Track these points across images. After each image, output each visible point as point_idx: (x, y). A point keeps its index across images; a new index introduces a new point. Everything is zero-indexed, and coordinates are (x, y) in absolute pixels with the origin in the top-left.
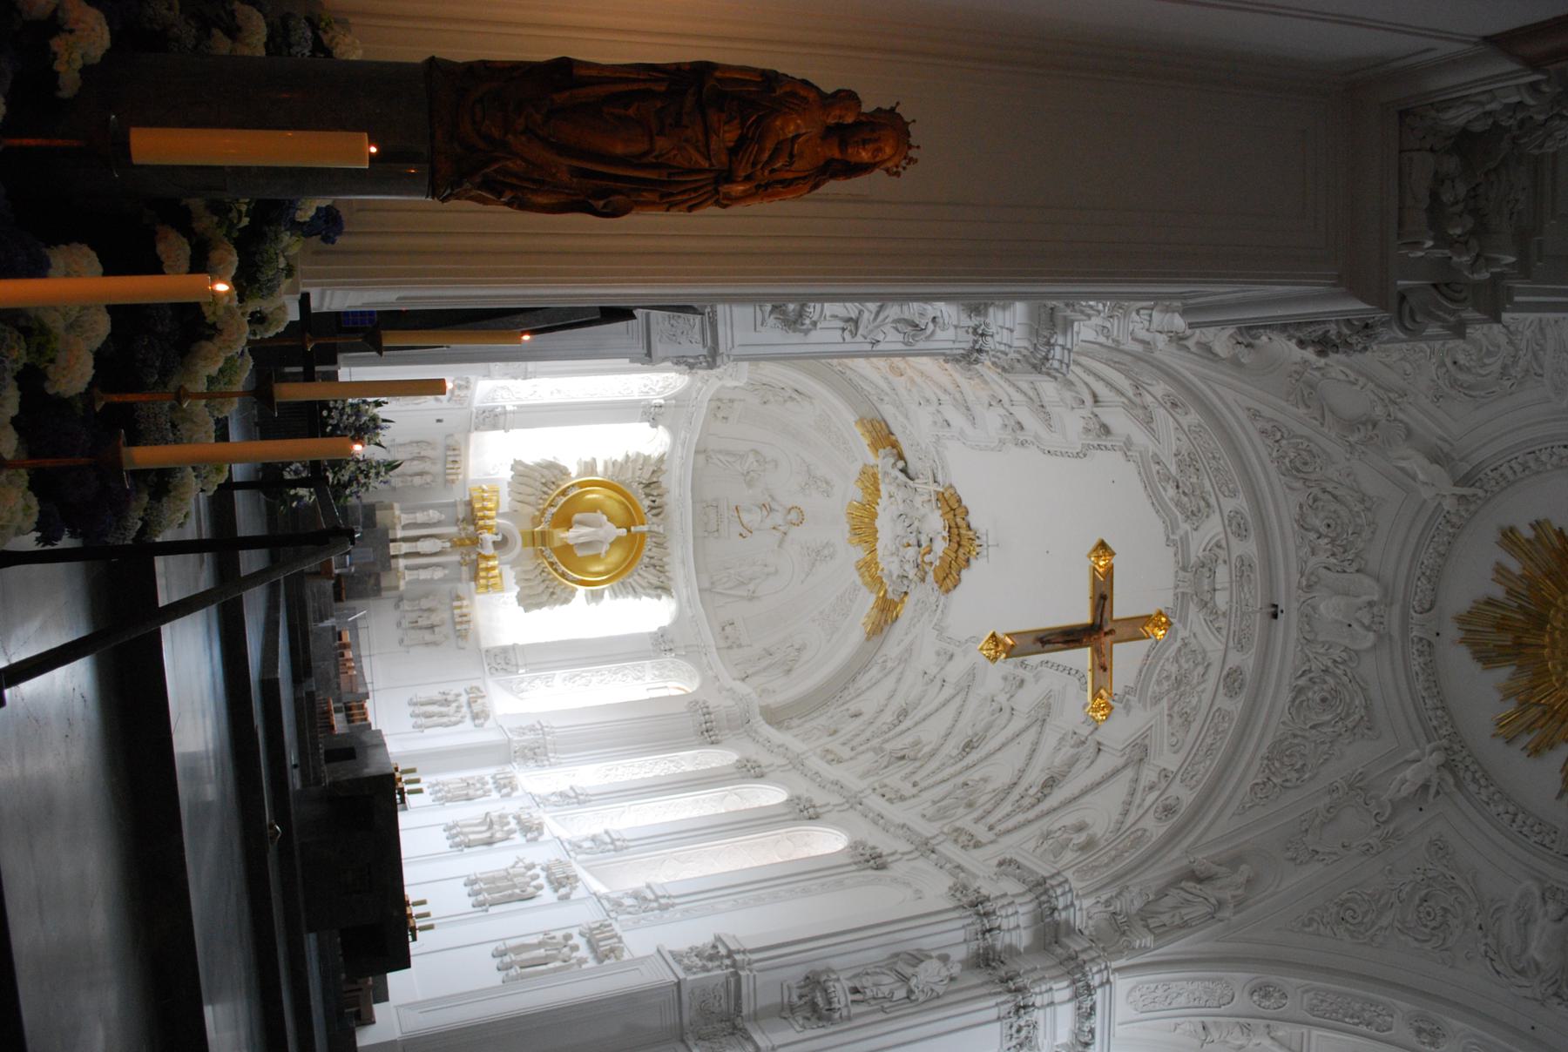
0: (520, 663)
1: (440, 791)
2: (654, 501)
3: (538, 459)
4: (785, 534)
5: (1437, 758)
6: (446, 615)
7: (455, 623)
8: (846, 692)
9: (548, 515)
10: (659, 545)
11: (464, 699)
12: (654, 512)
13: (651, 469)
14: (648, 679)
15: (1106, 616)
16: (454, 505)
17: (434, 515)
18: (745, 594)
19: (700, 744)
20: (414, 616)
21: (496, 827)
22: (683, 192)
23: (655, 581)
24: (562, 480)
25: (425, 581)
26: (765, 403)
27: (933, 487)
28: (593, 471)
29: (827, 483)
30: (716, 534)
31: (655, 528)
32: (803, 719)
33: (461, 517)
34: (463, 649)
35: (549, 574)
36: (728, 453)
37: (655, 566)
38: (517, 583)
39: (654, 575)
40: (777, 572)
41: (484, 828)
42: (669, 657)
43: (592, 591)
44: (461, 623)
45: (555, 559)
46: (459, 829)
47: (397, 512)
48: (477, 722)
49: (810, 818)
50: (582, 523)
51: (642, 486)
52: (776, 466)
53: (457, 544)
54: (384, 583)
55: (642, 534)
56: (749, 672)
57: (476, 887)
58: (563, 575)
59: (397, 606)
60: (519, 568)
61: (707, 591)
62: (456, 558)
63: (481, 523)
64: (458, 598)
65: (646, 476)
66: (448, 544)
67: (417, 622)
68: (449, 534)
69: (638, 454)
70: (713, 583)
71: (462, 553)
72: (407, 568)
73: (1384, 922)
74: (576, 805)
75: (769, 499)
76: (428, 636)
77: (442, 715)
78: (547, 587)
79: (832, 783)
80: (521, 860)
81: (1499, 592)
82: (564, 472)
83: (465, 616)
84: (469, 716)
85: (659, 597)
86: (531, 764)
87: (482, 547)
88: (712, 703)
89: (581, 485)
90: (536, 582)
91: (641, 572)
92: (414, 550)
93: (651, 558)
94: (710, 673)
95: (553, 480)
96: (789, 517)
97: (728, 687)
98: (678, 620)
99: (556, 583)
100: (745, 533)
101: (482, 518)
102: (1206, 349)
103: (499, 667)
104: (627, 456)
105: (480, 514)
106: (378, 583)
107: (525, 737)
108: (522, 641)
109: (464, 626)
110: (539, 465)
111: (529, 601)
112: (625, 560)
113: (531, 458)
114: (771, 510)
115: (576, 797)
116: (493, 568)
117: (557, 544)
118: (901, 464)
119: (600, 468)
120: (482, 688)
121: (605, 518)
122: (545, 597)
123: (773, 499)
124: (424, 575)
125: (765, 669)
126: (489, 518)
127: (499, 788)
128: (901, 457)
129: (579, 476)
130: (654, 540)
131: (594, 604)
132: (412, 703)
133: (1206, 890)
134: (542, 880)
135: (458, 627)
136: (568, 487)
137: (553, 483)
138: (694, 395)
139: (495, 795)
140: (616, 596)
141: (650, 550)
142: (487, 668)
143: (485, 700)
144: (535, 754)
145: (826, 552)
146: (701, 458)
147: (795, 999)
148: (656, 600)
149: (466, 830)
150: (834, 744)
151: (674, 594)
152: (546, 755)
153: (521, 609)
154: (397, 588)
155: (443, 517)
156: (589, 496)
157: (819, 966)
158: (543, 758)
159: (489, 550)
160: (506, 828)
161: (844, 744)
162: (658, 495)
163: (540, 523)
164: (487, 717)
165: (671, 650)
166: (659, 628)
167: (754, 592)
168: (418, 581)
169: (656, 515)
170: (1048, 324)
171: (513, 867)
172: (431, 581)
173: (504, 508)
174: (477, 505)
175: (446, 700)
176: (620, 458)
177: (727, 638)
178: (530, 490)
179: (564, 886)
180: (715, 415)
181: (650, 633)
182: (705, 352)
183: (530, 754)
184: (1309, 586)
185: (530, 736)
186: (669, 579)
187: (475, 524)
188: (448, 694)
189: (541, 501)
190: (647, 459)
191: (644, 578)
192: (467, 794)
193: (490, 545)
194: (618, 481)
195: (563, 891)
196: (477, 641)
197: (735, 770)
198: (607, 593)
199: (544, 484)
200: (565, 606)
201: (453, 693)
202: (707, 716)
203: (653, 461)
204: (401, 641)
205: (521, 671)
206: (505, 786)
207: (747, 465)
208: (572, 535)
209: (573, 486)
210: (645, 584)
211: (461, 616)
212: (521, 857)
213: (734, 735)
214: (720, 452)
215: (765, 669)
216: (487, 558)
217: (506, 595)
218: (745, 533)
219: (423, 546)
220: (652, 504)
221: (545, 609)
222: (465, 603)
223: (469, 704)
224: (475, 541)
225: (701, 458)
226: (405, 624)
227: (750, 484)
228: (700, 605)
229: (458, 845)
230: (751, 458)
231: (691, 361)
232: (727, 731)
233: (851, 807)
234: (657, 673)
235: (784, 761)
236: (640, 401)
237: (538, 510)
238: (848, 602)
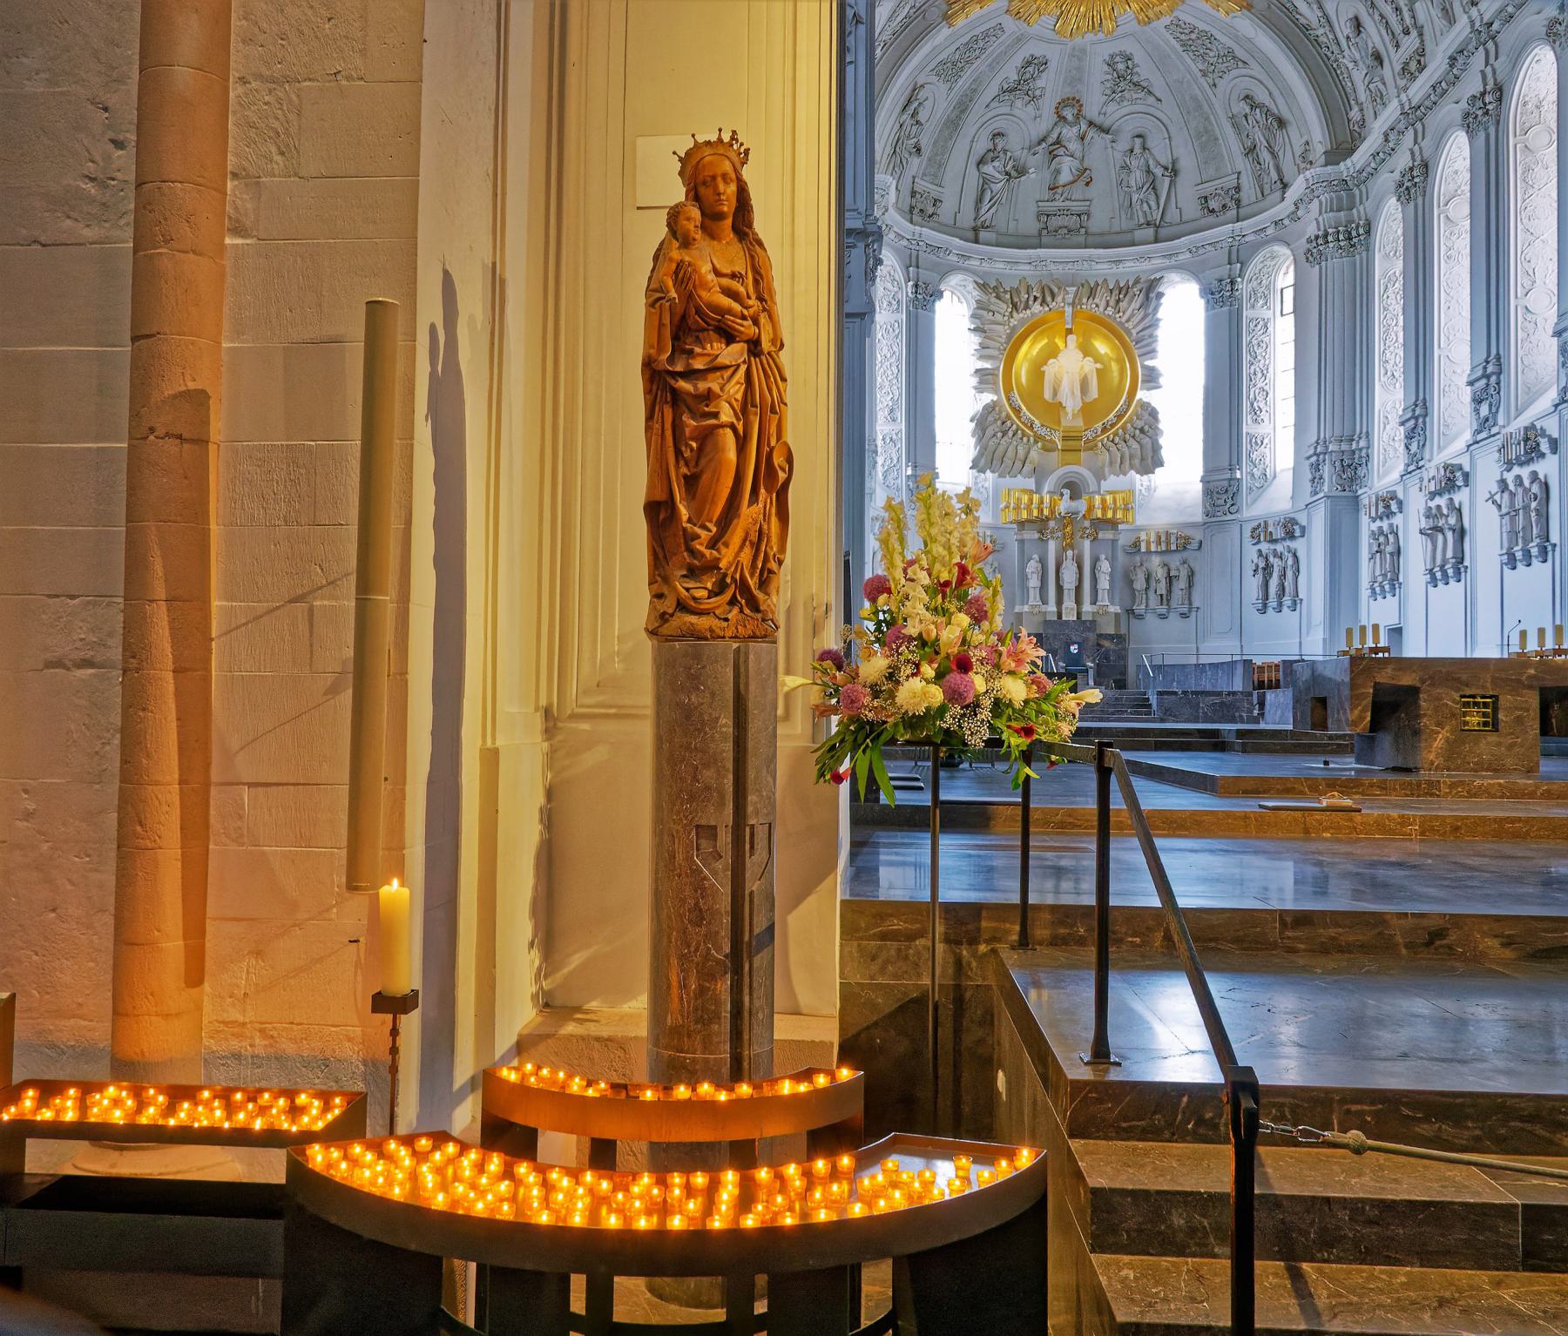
0: (1228, 476)
1: (1382, 587)
2: (1036, 298)
3: (973, 441)
4: (1091, 123)
6: (1156, 560)
7: (1168, 551)
8: (1323, 39)
9: (1043, 432)
10: (1092, 293)
11: (1264, 547)
12: (1049, 299)
13: (994, 300)
14: (1268, 314)
16: (1022, 542)
17: (1032, 567)
18: (1167, 180)
19: (1368, 250)
20: (1154, 601)
21: (1441, 523)
22: (770, 390)
23: (1136, 304)
24: (1000, 412)
25: (1112, 582)
26: (919, 150)
29: (1029, 63)
30: (1084, 217)
31: (1070, 298)
32: (1353, 102)
33: (1036, 536)
34: (1201, 543)
35: (1116, 434)
36: (979, 200)
37: (1118, 301)
38: (1125, 474)
39: (1130, 302)
40: (1138, 136)
41: (1440, 537)
42: (1243, 287)
43: (1142, 381)
44: (1168, 543)
45: (1099, 426)
46: (1437, 569)
47: (1026, 608)
48: (1297, 533)
49: (1500, 100)
50: (1055, 393)
51: (1015, 314)
52: (999, 134)
53: (1069, 544)
54: (1111, 631)
55: (1074, 315)
56: (1274, 176)
57: (1519, 555)
58: (1119, 416)
59: (1140, 617)
60: (1107, 470)
61: (1159, 231)
62: (1087, 543)
63: (1046, 512)
64: (1137, 544)
65: (1004, 307)
66: (1070, 553)
67: (1161, 595)
68: (1057, 552)
69: (974, 316)
70: (1148, 224)
71: (1082, 537)
72: (1094, 602)
74: (1428, 419)
75: (1044, 145)
76: (1181, 584)
77: (1283, 575)
78: (1133, 437)
79: (1452, 66)
80: (1492, 496)
83: (1160, 537)
84: (1288, 543)
85: (1160, 295)
86: (1361, 472)
87: (1077, 513)
88: (1312, 230)
90: (1126, 450)
91: (1124, 320)
92: (1073, 594)
93: (1108, 305)
94: (1270, 231)
95: (999, 423)
96: (1070, 117)
97: (1293, 208)
98: (1192, 270)
99: (1129, 425)
100: (1084, 179)
101: (1041, 511)
103: (1230, 502)
104: (975, 330)
105: (1035, 513)
106: (1110, 637)
107: (1326, 476)
108: (1199, 471)
109: (1173, 539)
110: (979, 440)
111: (1150, 460)
112: (1106, 338)
114: (1058, 142)
115: (1417, 418)
116: (1104, 501)
117: (1080, 423)
119: (987, 365)
120: (1255, 524)
121: (1051, 361)
122: (1146, 440)
123: (1043, 140)
124: (1104, 583)
125: (1274, 155)
126: (1041, 502)
127: (1389, 514)
129: (996, 392)
130: (1084, 300)
131: (1162, 381)
132: (1263, 610)
134: (1525, 472)
135: (1173, 547)
136: (1010, 405)
137: (1003, 423)
138: (905, 243)
139: (1398, 520)
140: (1154, 351)
141: (1097, 306)
142: (1229, 517)
143: (1270, 522)
144: (1349, 466)
145: (1121, 67)
146: (983, 235)
148: (1163, 300)
149: (1439, 562)
150: (1395, 59)
151: (1158, 276)
152: (1353, 452)
153: (1158, 470)
154: (1117, 615)
155: (1036, 557)
156: (1023, 380)
158: (1357, 456)
159: (1081, 506)
160: (1445, 511)
161: (1397, 46)
162: (1028, 293)
163: (1051, 441)
164: (1294, 522)
165: (1232, 283)
166: (1202, 297)
167: (1166, 169)
168: (1111, 591)
169: (1053, 296)
171: (1499, 507)
172: (1111, 575)
173: (1031, 483)
174: (1025, 515)
175: (1264, 569)
176: (974, 340)
177: (1224, 206)
178: (1010, 453)
179: (1538, 445)
180: (930, 216)
181: (1207, 310)
182: (861, 245)
183: (1349, 473)
185: (1326, 470)
186: (1137, 281)
187: (1048, 519)
188: (1257, 566)
189: (1025, 439)
190: (980, 305)
191: (1133, 315)
192: (1392, 554)
193: (1074, 504)
194: (1007, 343)
195: (1544, 446)
196: (1193, 525)
197: (1412, 203)
198: (1149, 363)
199: (1004, 433)
200: (1160, 416)
201: (1256, 561)
202: (1330, 238)
203: (985, 298)
204: (1184, 616)
205: (1238, 476)
206: (1388, 507)
207: (997, 175)
208: (1072, 404)
209: (1008, 399)
210: (1142, 313)
211: (1159, 543)
212: (1489, 496)
213: (1361, 203)
214: (977, 209)
215: (1274, 155)
216: (1091, 508)
217: (1138, 487)
218: (1084, 179)
220: (1039, 301)
221: (1162, 441)
222: (1143, 536)
223: (1275, 541)
224: (1070, 519)
225: (983, 235)
226: (1163, 609)
227: (1021, 171)
228: (1176, 241)
229: (1458, 573)
230: (988, 169)
231: (871, 262)
232: (1354, 211)
233: (1493, 38)
234: (1261, 302)
235: (1410, 134)
236: (909, 313)
237: (1036, 442)
238: (1193, 36)
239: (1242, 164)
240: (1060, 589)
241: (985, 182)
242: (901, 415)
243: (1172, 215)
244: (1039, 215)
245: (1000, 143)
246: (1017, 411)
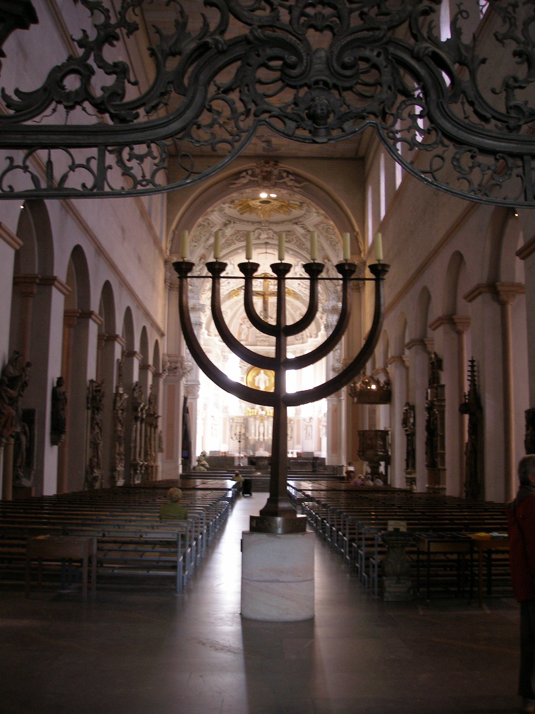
5: (295, 226)
15: (261, 293)
50: (258, 383)
73: (333, 238)
102: (200, 269)
119: (242, 376)
170: (194, 309)
176: (240, 369)
184: (259, 239)
187: (257, 415)
216: (266, 413)
219: (262, 432)
224: (261, 416)
230: (243, 326)
240: (259, 433)
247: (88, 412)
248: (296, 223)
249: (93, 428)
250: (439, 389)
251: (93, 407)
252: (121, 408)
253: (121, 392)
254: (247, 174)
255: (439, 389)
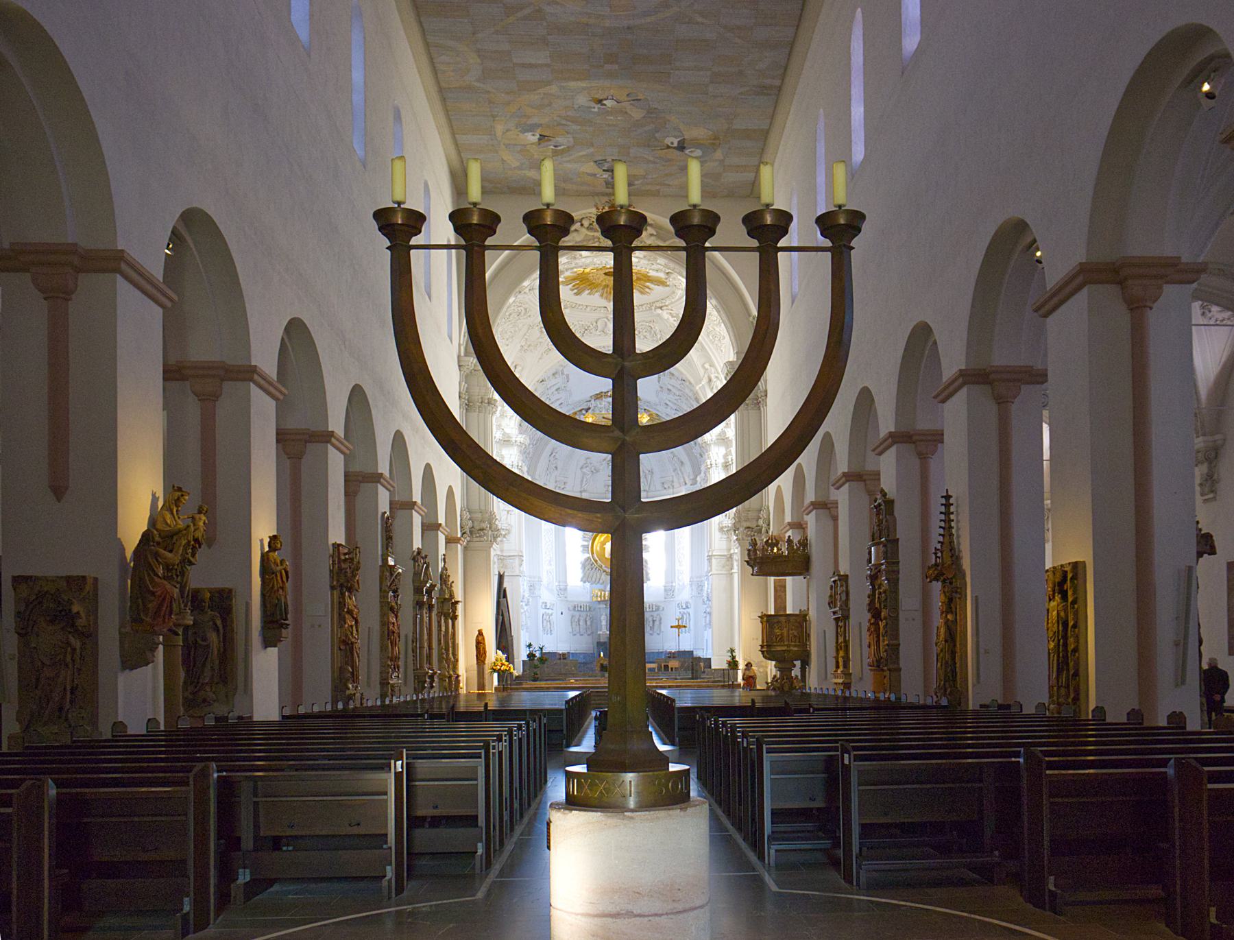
5: (659, 311)
26: (556, 468)
27: (593, 402)
28: (587, 546)
36: (582, 481)
81: (597, 294)
82: (589, 558)
89: (592, 553)
101: (604, 597)
108: (664, 584)
113: (580, 574)
118: (584, 412)
119: (586, 543)
128: (581, 410)
133: (714, 379)
147: (725, 536)
156: (598, 548)
157: (717, 527)
174: (599, 599)
178: (595, 576)
214: (581, 485)
230: (584, 470)
239: (673, 474)
241: (584, 474)
242: (553, 563)
243: (652, 488)
244: (605, 486)
245: (588, 461)
246: (596, 561)
247: (332, 595)
248: (661, 308)
249: (342, 620)
250: (889, 545)
251: (342, 586)
252: (393, 587)
253: (391, 562)
254: (582, 225)
255: (889, 545)
